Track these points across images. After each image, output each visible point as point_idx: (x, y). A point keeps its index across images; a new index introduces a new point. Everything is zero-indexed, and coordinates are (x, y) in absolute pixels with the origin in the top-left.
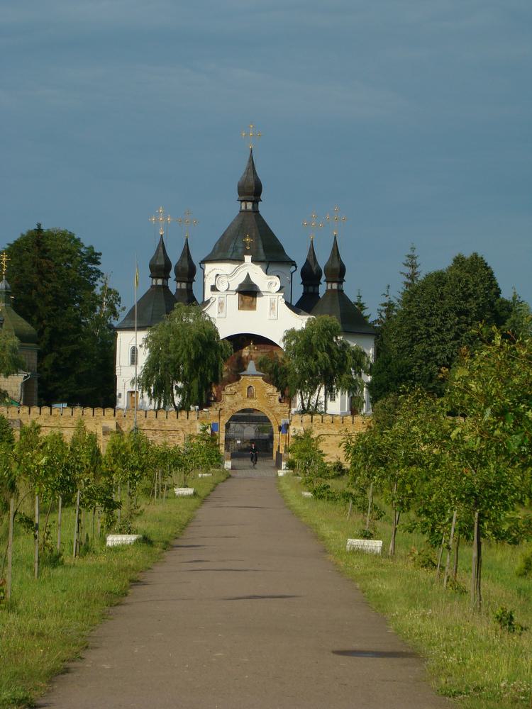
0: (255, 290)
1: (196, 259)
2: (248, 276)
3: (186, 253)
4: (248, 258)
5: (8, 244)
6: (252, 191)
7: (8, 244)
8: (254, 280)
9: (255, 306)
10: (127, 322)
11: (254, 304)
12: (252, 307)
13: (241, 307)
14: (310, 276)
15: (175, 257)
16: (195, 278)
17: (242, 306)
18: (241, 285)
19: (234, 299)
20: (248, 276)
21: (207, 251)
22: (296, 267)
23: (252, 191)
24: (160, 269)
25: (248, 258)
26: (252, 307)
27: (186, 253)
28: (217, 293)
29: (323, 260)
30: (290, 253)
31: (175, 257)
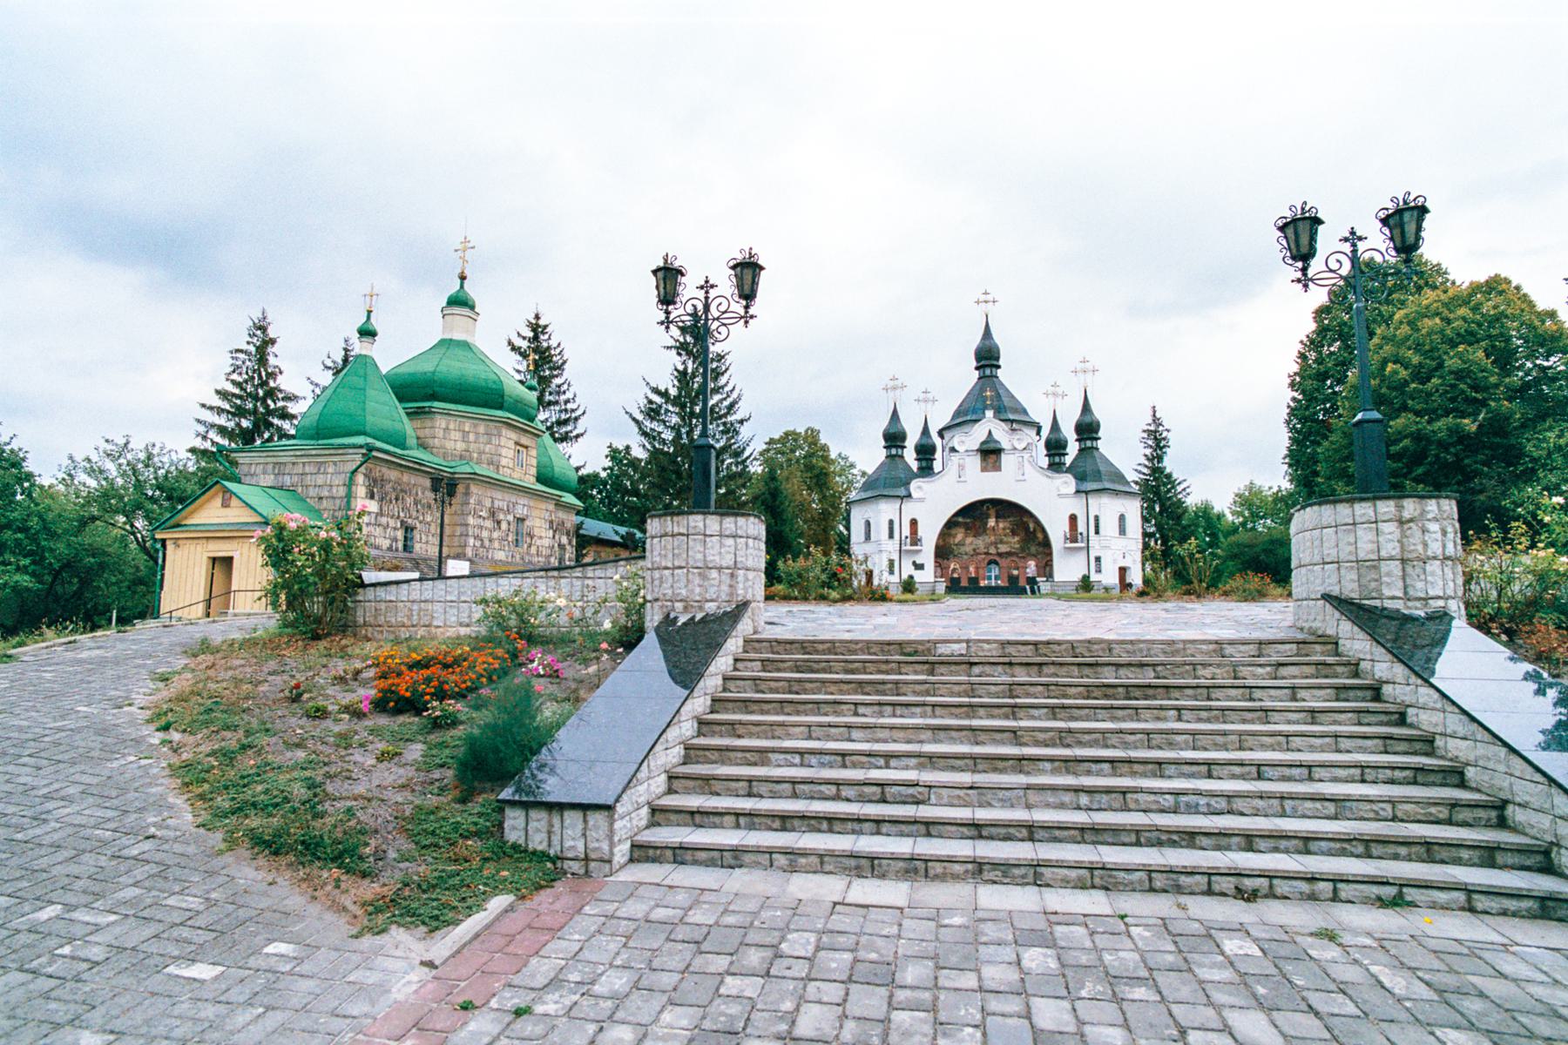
2: (990, 432)
4: (989, 414)
6: (987, 357)
8: (997, 435)
12: (997, 468)
13: (984, 469)
14: (1055, 447)
17: (984, 469)
18: (983, 443)
19: (976, 461)
20: (990, 432)
21: (945, 419)
23: (987, 357)
24: (894, 439)
25: (989, 414)
26: (997, 468)
30: (1035, 416)
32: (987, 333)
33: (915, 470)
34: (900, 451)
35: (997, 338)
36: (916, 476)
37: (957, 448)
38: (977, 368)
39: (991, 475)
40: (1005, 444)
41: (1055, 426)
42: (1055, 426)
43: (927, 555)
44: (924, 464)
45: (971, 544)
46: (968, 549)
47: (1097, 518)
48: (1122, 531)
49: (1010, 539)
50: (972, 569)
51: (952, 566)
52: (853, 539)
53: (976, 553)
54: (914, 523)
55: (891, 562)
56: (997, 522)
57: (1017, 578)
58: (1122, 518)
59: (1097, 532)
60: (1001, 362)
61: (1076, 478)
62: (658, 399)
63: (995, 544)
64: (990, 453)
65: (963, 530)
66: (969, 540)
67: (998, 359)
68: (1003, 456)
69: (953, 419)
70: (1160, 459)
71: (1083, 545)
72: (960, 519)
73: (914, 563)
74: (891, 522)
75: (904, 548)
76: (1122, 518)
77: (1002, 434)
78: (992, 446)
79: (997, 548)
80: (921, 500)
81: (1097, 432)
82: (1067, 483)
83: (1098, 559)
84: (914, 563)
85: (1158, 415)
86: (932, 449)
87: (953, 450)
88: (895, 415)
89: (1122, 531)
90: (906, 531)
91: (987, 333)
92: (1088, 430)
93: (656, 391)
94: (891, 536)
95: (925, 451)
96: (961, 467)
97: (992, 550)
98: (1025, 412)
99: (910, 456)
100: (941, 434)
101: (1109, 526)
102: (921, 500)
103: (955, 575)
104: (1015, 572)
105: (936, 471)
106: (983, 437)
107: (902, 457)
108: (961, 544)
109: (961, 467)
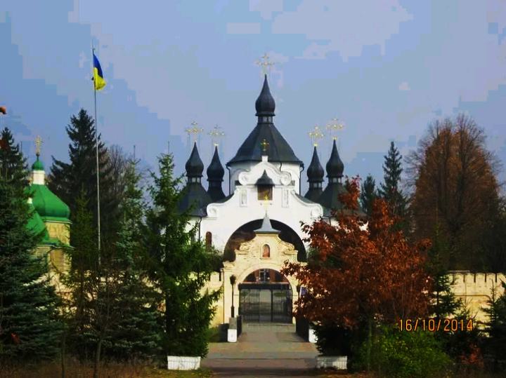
0: (271, 183)
1: (224, 162)
2: (265, 173)
3: (216, 159)
4: (265, 158)
6: (265, 107)
12: (270, 198)
13: (261, 198)
14: (314, 174)
15: (206, 161)
16: (224, 178)
17: (261, 198)
18: (260, 180)
19: (255, 194)
20: (265, 173)
23: (265, 107)
25: (265, 158)
27: (216, 159)
28: (240, 186)
29: (324, 161)
30: (299, 154)
31: (206, 161)
32: (265, 89)
34: (198, 179)
35: (274, 94)
37: (241, 182)
40: (275, 180)
41: (315, 159)
42: (315, 159)
44: (214, 185)
60: (276, 112)
61: (323, 205)
62: (59, 167)
64: (264, 187)
68: (273, 188)
70: (395, 183)
72: (242, 232)
77: (273, 175)
78: (262, 183)
80: (214, 219)
85: (395, 148)
86: (222, 172)
87: (238, 183)
91: (265, 89)
92: (335, 167)
93: (58, 163)
95: (216, 174)
96: (244, 196)
98: (292, 153)
99: (205, 183)
102: (214, 219)
105: (227, 194)
106: (260, 175)
107: (200, 184)
109: (244, 196)
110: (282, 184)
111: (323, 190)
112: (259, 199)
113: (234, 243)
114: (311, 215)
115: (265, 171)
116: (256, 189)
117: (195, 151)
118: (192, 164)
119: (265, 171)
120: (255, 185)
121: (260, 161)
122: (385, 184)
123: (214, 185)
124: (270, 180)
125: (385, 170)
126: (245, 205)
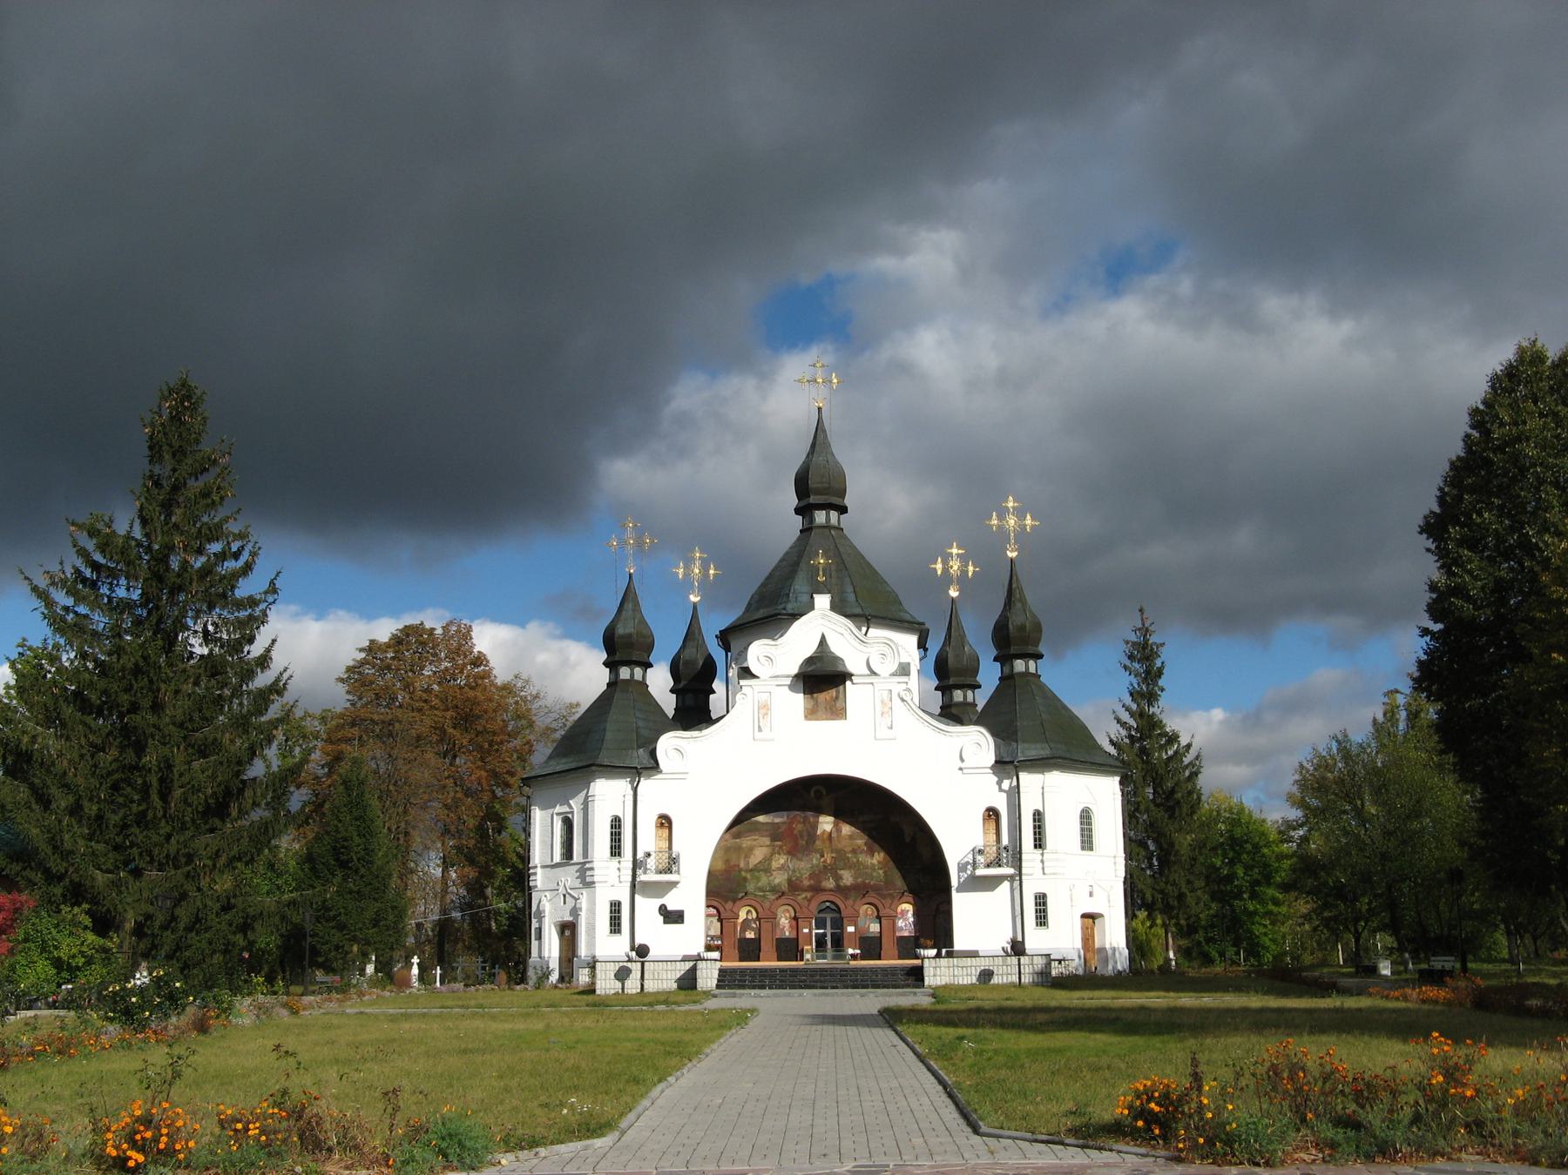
2: (823, 641)
3: (693, 634)
4: (822, 601)
5: (361, 650)
7: (361, 650)
8: (837, 647)
9: (844, 709)
10: (552, 762)
11: (839, 704)
12: (837, 711)
13: (811, 714)
17: (811, 714)
18: (810, 661)
20: (823, 641)
22: (926, 650)
25: (822, 601)
26: (837, 711)
31: (667, 643)
33: (670, 712)
34: (638, 671)
36: (667, 725)
38: (798, 511)
39: (826, 728)
43: (690, 894)
45: (782, 868)
46: (779, 879)
47: (1038, 817)
48: (1087, 842)
49: (862, 858)
50: (784, 922)
51: (743, 915)
52: (537, 856)
53: (794, 886)
54: (665, 822)
55: (615, 907)
56: (836, 825)
57: (878, 940)
58: (1086, 817)
59: (1039, 843)
63: (831, 870)
65: (767, 841)
66: (781, 860)
67: (842, 493)
69: (747, 610)
71: (1010, 871)
72: (761, 818)
73: (663, 910)
74: (616, 823)
75: (642, 877)
76: (1086, 817)
79: (838, 878)
81: (1037, 642)
82: (978, 744)
83: (1041, 900)
84: (663, 910)
88: (629, 597)
89: (1087, 842)
90: (649, 839)
94: (616, 850)
97: (830, 883)
99: (659, 681)
100: (725, 638)
101: (1064, 831)
102: (681, 775)
103: (750, 935)
104: (874, 928)
105: (714, 716)
106: (810, 649)
108: (764, 867)
109: (764, 709)
110: (873, 673)
111: (979, 708)
112: (806, 718)
113: (739, 849)
114: (962, 760)
115: (823, 637)
116: (801, 686)
117: (629, 597)
118: (621, 630)
119: (823, 637)
120: (796, 676)
121: (810, 607)
122: (1134, 707)
123: (690, 701)
124: (837, 660)
125: (1125, 667)
126: (766, 733)
